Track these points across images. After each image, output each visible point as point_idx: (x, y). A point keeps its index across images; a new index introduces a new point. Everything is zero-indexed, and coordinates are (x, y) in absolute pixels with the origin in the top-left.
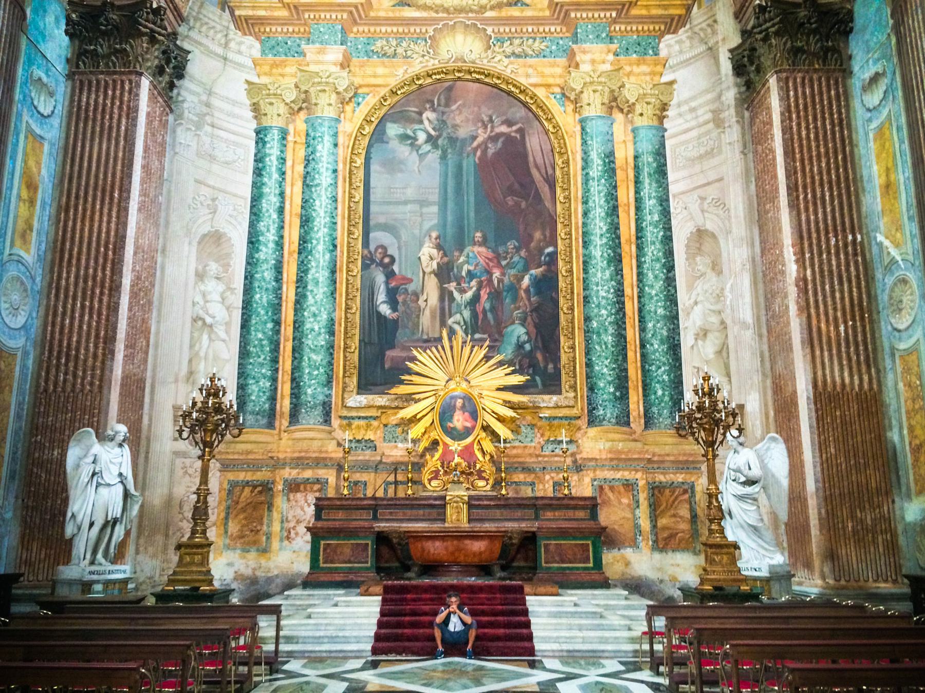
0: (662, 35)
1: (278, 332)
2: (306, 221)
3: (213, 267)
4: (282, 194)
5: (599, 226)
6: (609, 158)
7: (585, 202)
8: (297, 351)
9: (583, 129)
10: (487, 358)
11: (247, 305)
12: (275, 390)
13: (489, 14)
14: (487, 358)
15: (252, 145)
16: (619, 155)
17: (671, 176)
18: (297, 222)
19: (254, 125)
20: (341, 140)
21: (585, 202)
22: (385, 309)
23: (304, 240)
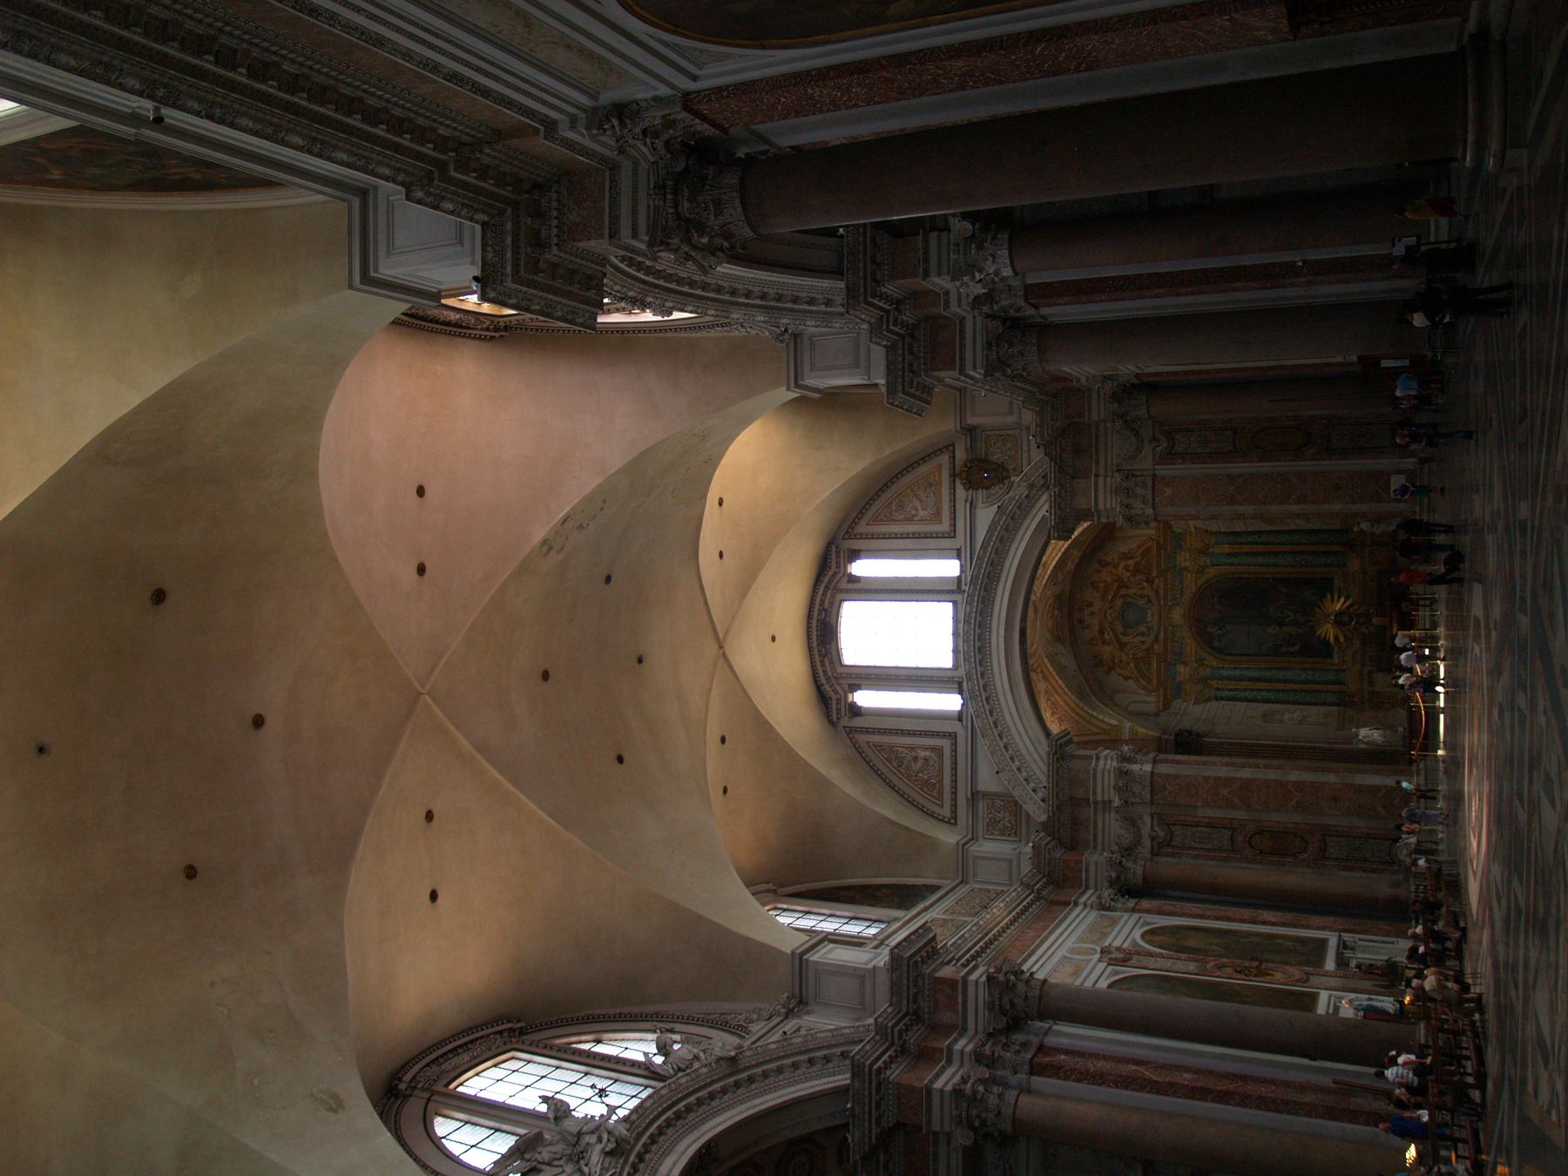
0: (1173, 531)
1: (1306, 691)
2: (1258, 680)
3: (1278, 717)
4: (1246, 690)
5: (1260, 560)
6: (1229, 555)
7: (1249, 565)
8: (1313, 682)
9: (1217, 565)
10: (1319, 607)
11: (1294, 703)
12: (1331, 692)
13: (1162, 603)
14: (1319, 607)
15: (1223, 702)
16: (1227, 550)
17: (1238, 530)
18: (1257, 684)
19: (1214, 702)
20: (1220, 665)
21: (1249, 565)
22: (1296, 648)
23: (1266, 681)
